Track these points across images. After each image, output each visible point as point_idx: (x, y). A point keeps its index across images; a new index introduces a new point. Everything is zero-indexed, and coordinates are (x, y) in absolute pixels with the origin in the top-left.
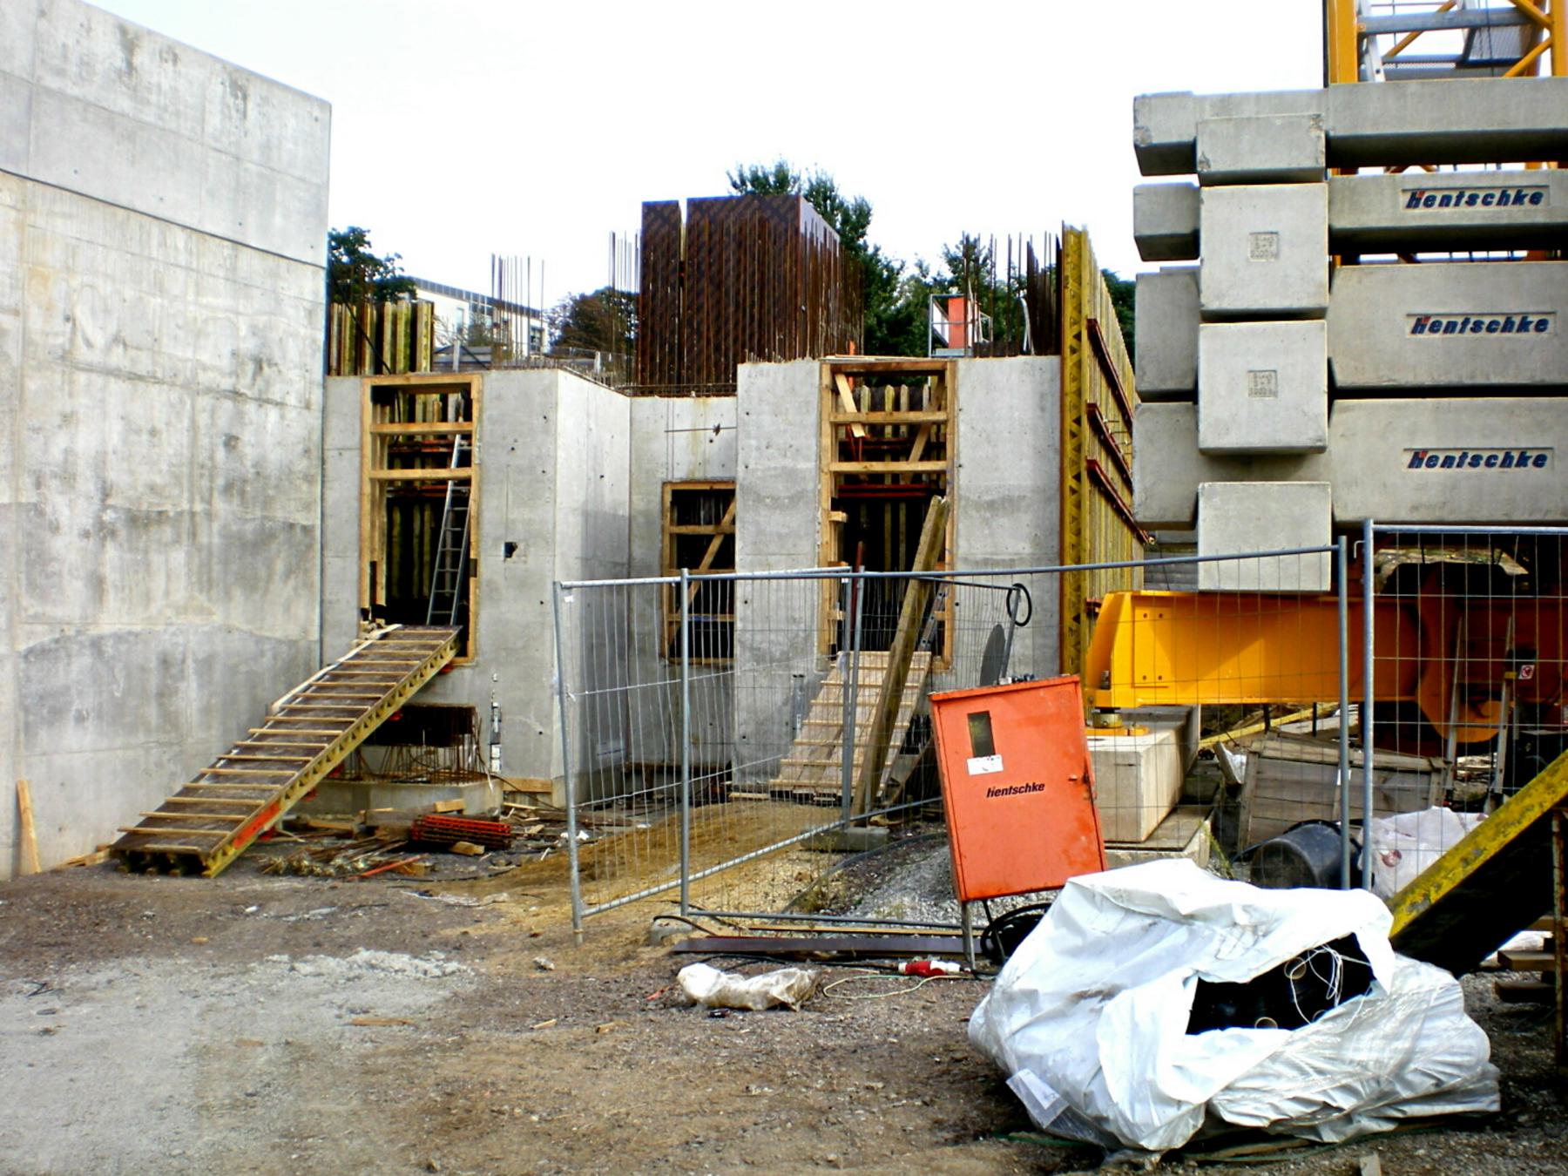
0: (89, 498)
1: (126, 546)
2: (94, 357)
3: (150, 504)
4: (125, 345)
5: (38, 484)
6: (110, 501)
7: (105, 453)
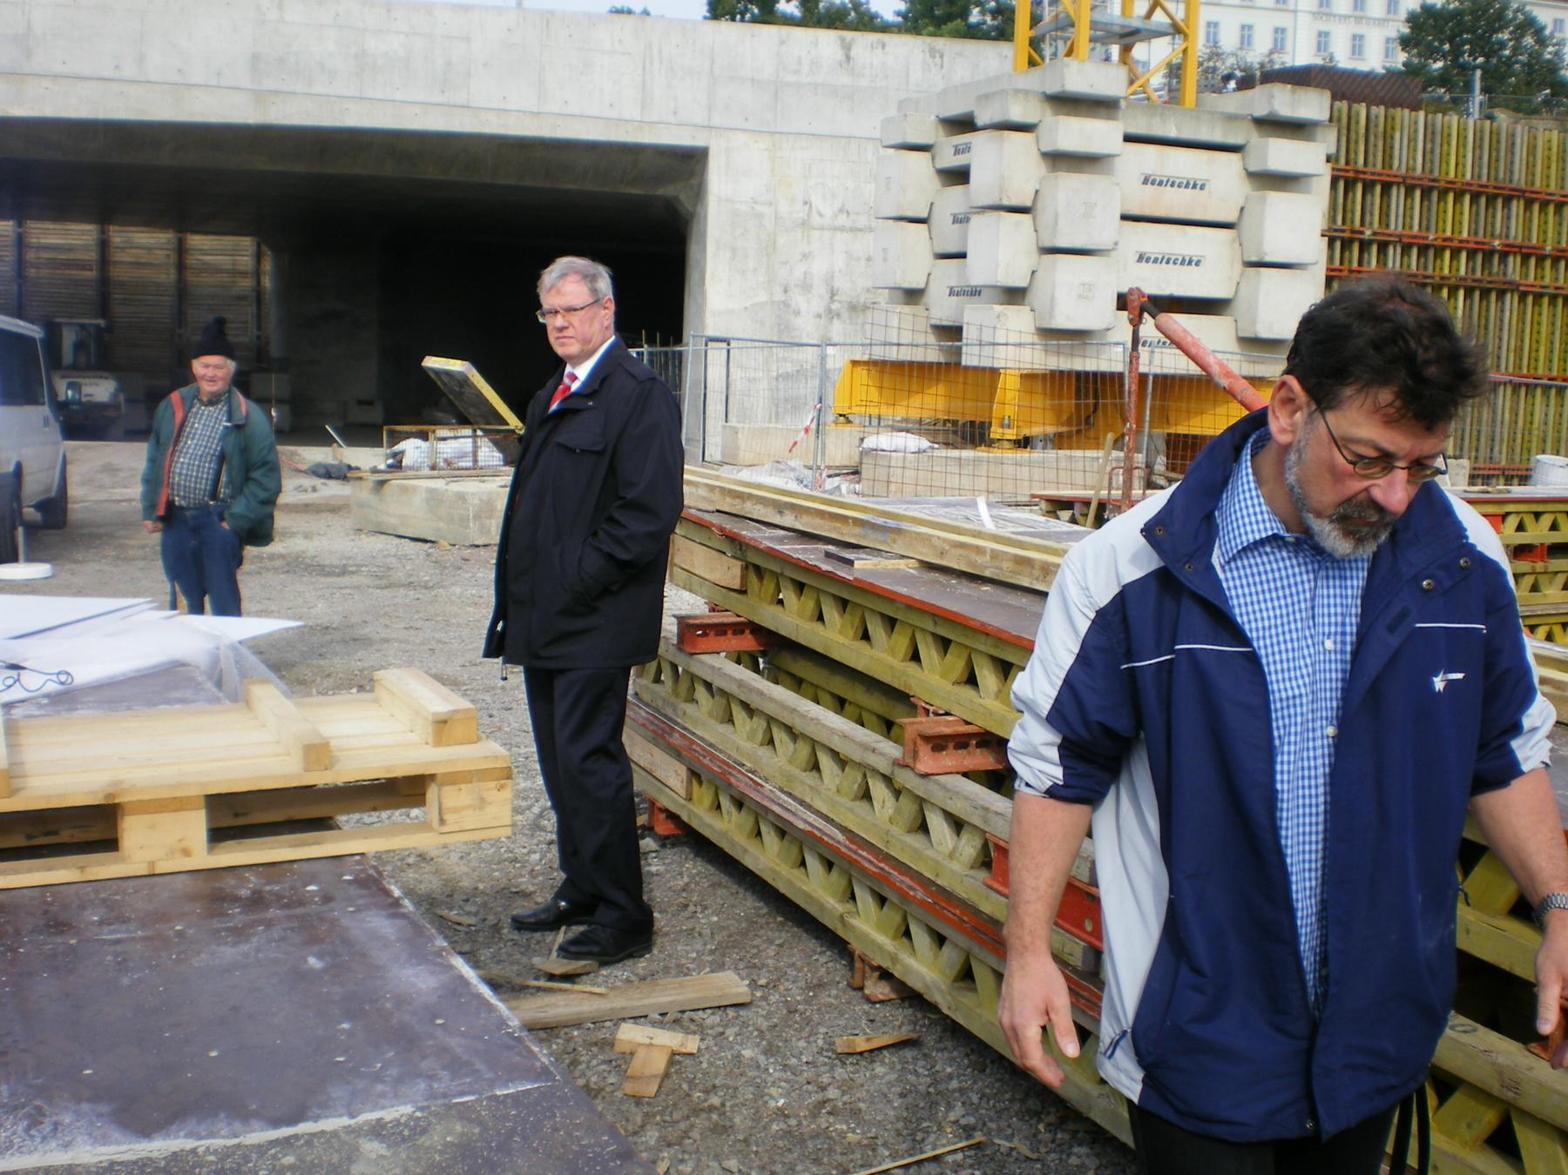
5: (786, 291)
6: (836, 298)
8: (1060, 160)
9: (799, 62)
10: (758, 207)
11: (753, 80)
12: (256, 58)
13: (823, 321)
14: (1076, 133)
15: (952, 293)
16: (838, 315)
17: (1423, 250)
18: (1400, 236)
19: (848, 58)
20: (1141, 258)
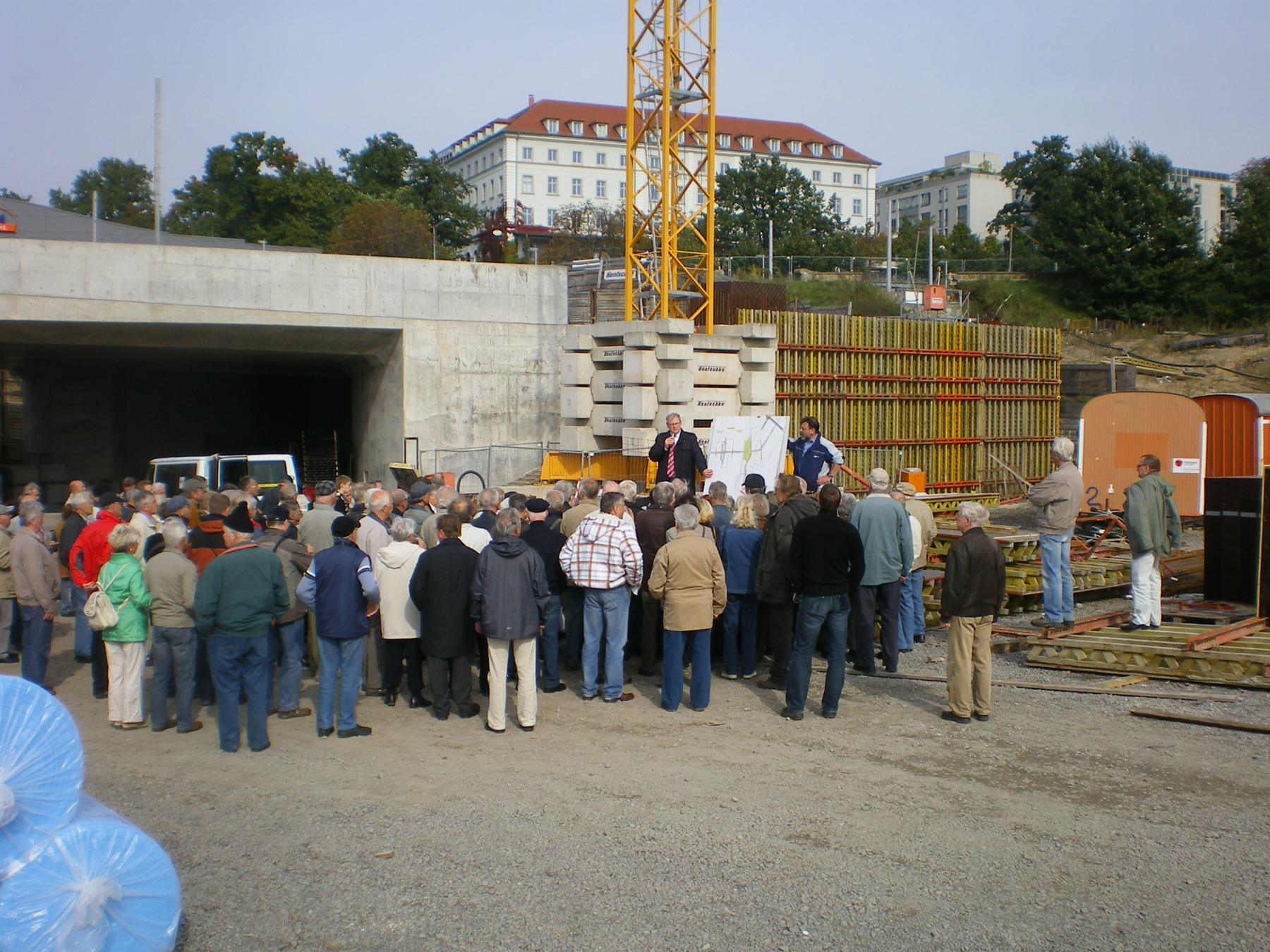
2: (468, 369)
8: (666, 363)
12: (151, 284)
13: (468, 425)
14: (674, 351)
15: (606, 420)
17: (800, 381)
19: (476, 277)
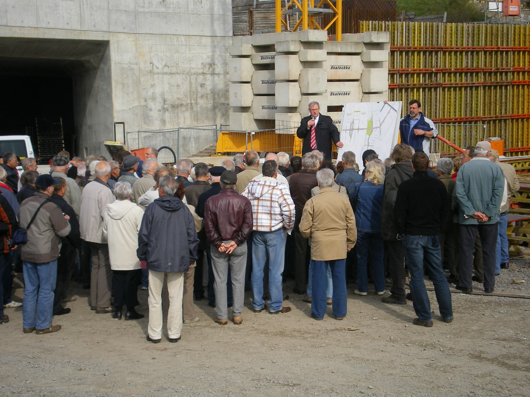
0: (160, 102)
1: (171, 112)
2: (160, 71)
3: (178, 102)
4: (168, 67)
5: (146, 101)
6: (166, 103)
7: (164, 92)
9: (144, 3)
10: (131, 66)
11: (125, 11)
13: (161, 113)
15: (263, 108)
16: (167, 110)
17: (407, 75)
18: (398, 71)
20: (332, 94)
